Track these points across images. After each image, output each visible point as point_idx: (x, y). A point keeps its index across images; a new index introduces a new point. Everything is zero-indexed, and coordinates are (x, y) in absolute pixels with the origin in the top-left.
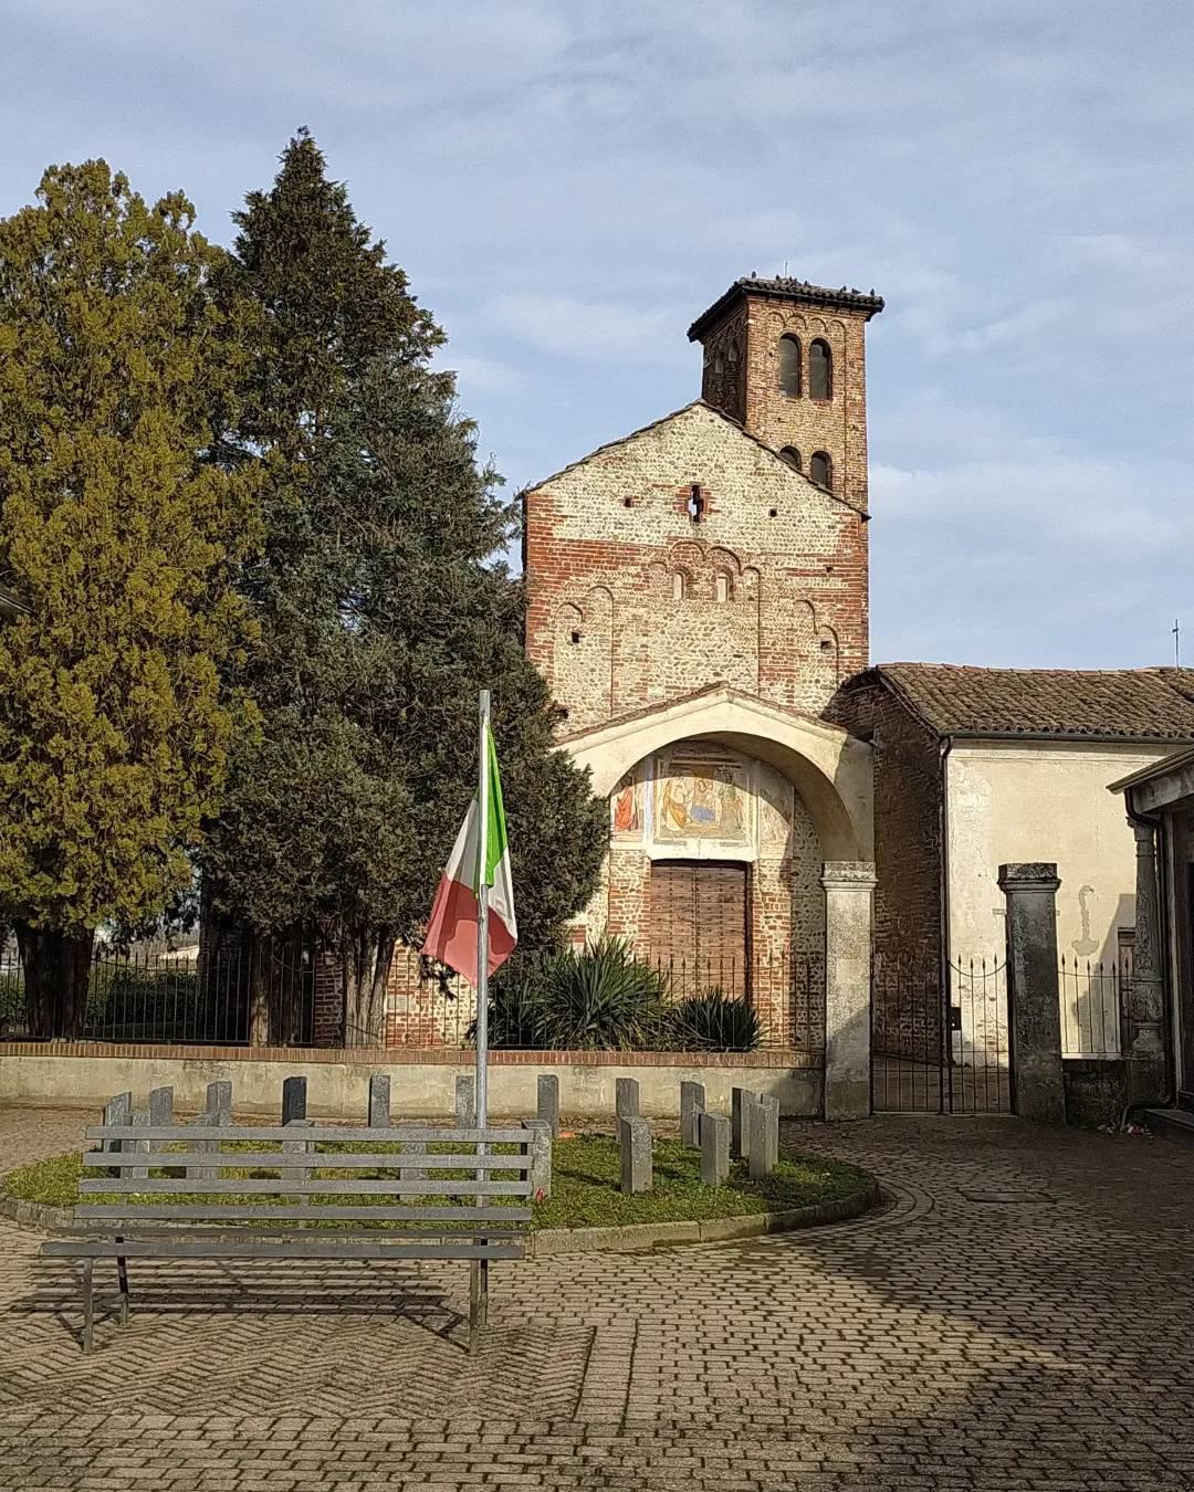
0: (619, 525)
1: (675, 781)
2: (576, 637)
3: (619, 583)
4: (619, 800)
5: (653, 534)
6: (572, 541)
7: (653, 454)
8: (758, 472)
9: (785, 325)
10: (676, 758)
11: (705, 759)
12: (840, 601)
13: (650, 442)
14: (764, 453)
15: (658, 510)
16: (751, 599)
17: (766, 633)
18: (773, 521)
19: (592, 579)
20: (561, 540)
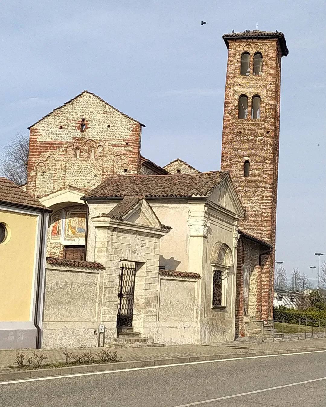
0: (58, 135)
1: (72, 219)
3: (57, 154)
4: (53, 226)
6: (43, 142)
10: (73, 211)
11: (83, 211)
12: (130, 155)
14: (107, 106)
15: (70, 129)
18: (108, 129)
19: (48, 154)
20: (40, 142)
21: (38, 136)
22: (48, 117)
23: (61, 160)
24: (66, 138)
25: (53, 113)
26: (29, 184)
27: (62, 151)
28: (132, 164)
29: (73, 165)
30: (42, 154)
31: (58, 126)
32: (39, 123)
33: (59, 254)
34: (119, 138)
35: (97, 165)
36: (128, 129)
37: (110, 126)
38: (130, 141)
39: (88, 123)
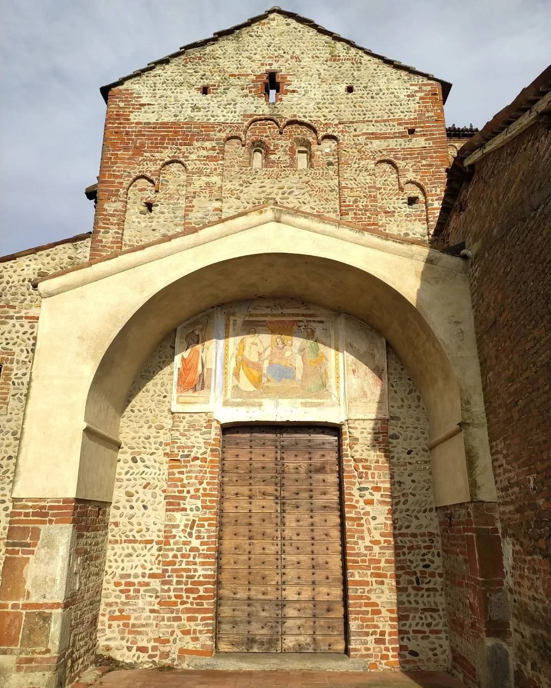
0: (195, 108)
1: (249, 339)
2: (149, 206)
4: (183, 359)
5: (230, 114)
6: (149, 123)
10: (251, 315)
11: (283, 315)
13: (228, 45)
14: (339, 45)
15: (233, 93)
16: (330, 164)
17: (346, 192)
20: (137, 123)
21: (133, 108)
23: (208, 171)
24: (221, 115)
26: (101, 234)
28: (434, 183)
29: (245, 185)
30: (145, 154)
31: (196, 87)
32: (138, 78)
33: (205, 453)
35: (321, 186)
36: (408, 96)
37: (355, 88)
38: (420, 123)
39: (289, 81)
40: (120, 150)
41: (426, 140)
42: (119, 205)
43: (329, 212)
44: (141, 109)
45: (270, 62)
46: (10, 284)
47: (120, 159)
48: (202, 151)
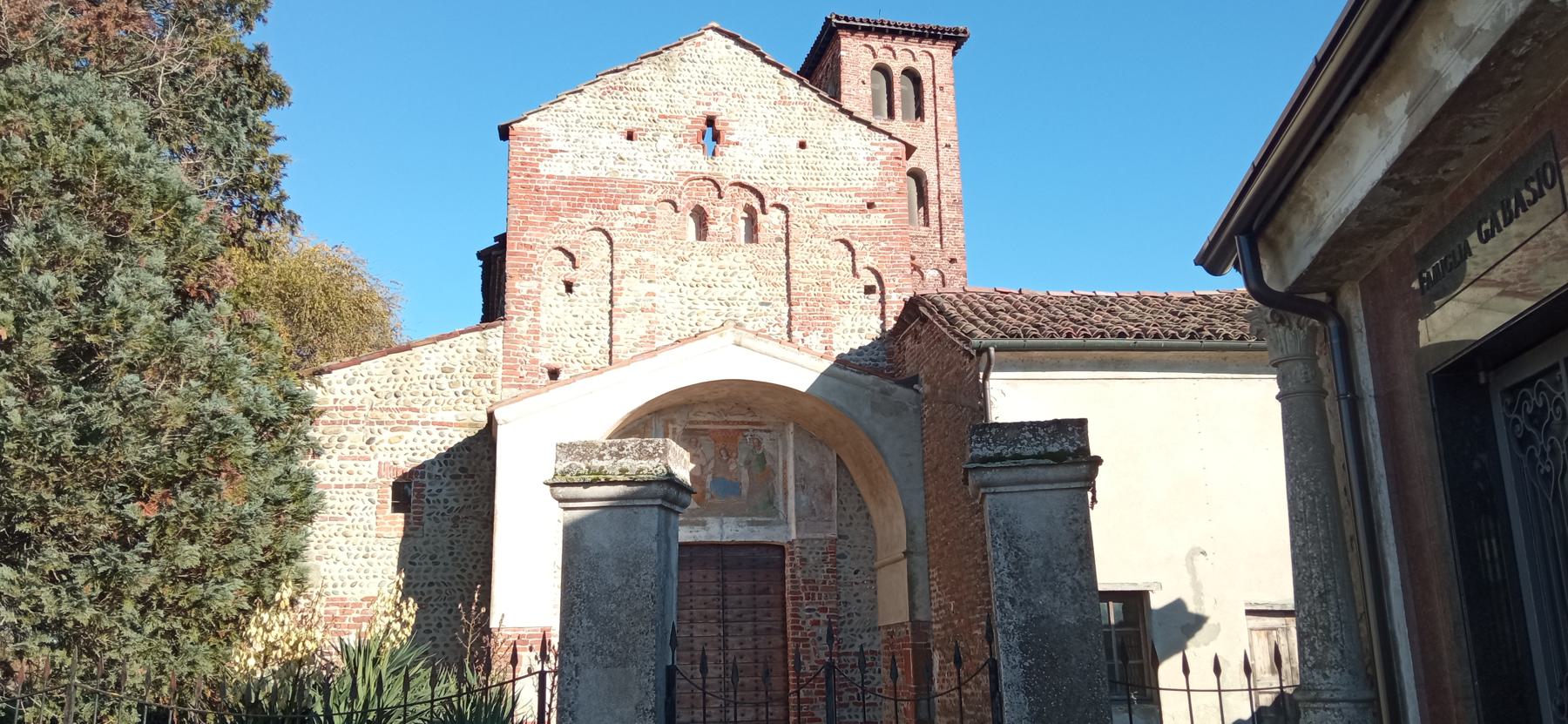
2: (569, 287)
3: (619, 224)
6: (563, 177)
7: (659, 84)
8: (784, 100)
9: (875, 55)
12: (885, 240)
15: (665, 142)
19: (588, 219)
20: (548, 177)
22: (577, 94)
25: (596, 84)
26: (514, 321)
27: (638, 212)
28: (892, 271)
30: (561, 219)
31: (618, 130)
34: (841, 186)
35: (769, 267)
36: (868, 159)
37: (808, 144)
40: (530, 212)
41: (886, 217)
42: (533, 285)
43: (777, 300)
44: (551, 156)
45: (708, 101)
46: (409, 382)
47: (532, 224)
48: (630, 217)
